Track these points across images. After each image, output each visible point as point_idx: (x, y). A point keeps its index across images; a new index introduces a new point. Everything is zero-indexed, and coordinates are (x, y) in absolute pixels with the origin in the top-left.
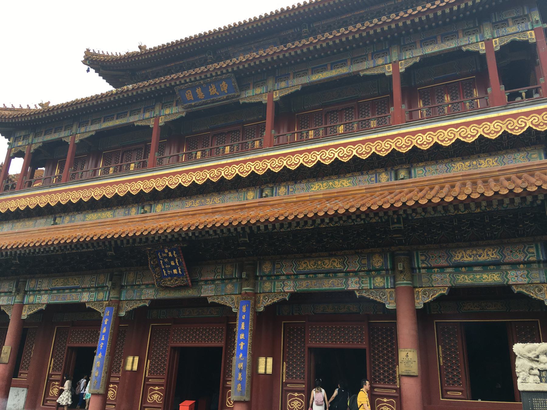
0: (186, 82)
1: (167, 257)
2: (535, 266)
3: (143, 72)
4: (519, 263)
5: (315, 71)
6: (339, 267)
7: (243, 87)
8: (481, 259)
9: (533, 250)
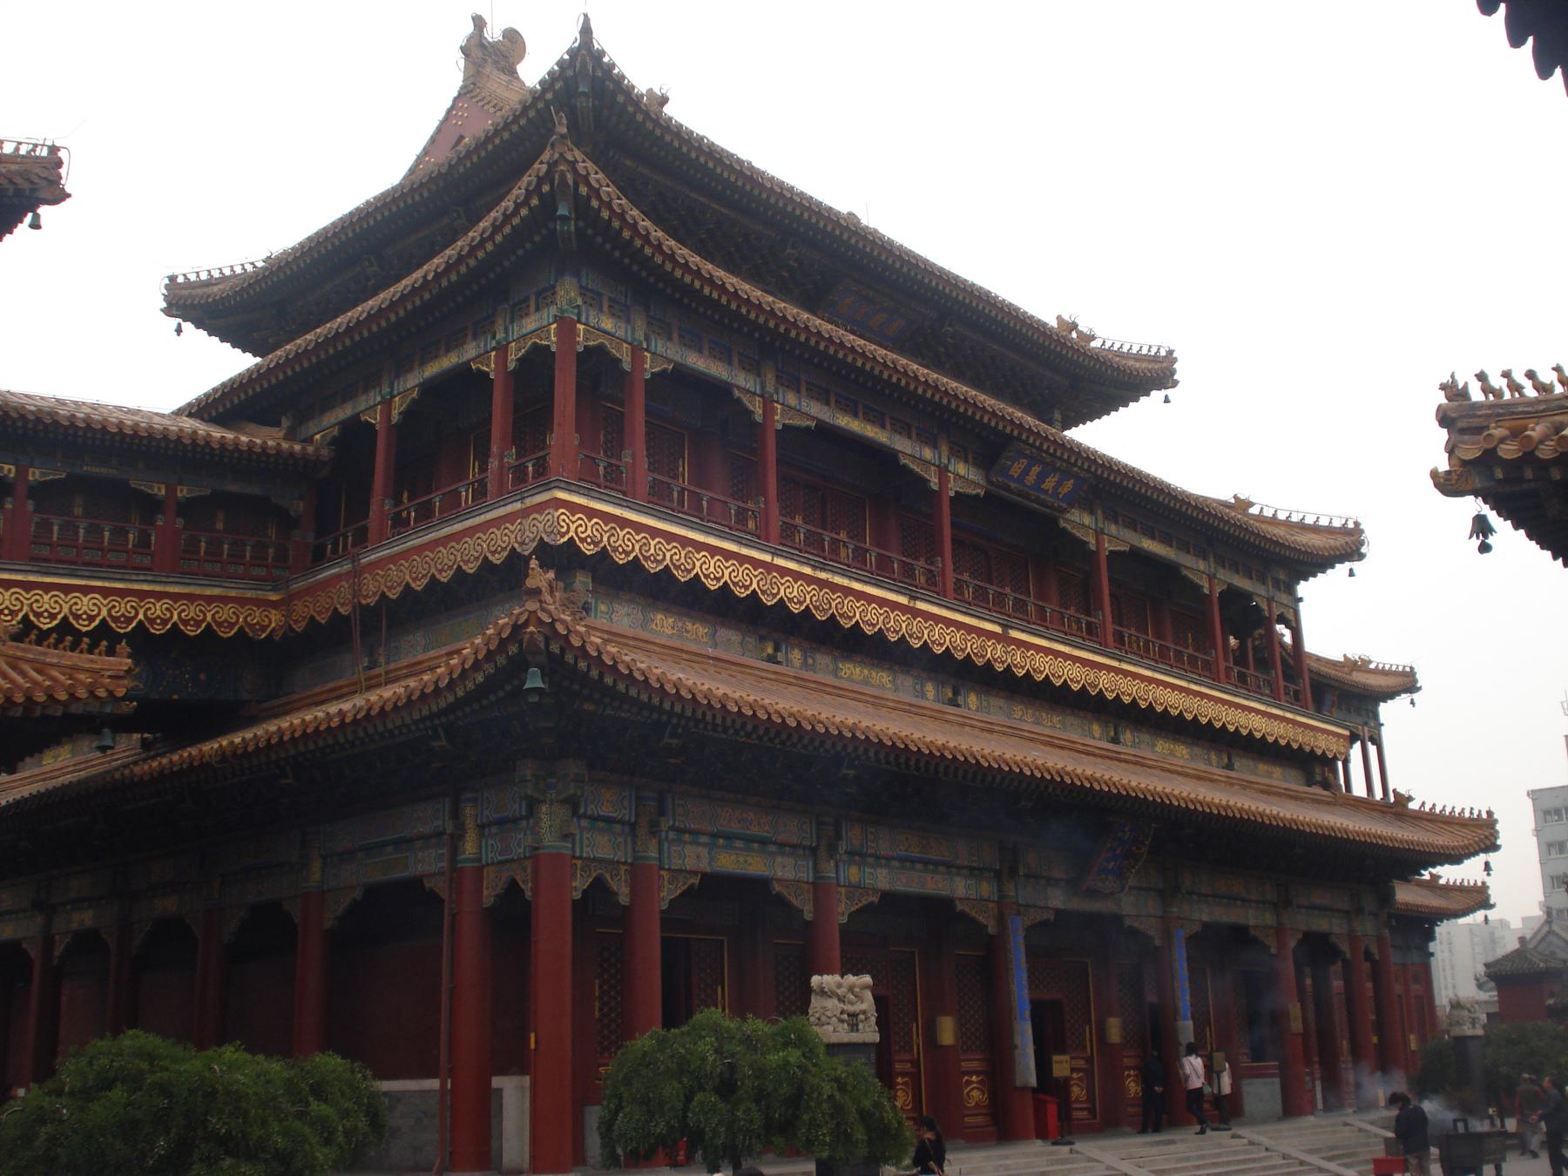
3: (628, 163)
7: (1074, 501)
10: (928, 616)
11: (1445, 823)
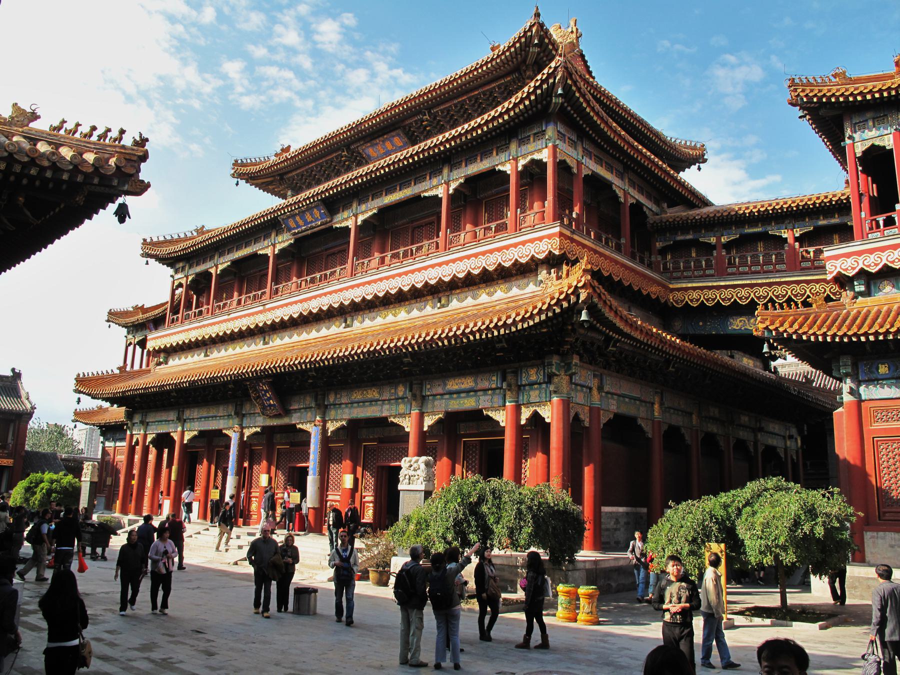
0: (285, 213)
1: (263, 390)
2: (498, 391)
4: (488, 390)
5: (390, 191)
6: (377, 396)
8: (463, 387)
9: (494, 378)
10: (236, 318)
11: (98, 380)
